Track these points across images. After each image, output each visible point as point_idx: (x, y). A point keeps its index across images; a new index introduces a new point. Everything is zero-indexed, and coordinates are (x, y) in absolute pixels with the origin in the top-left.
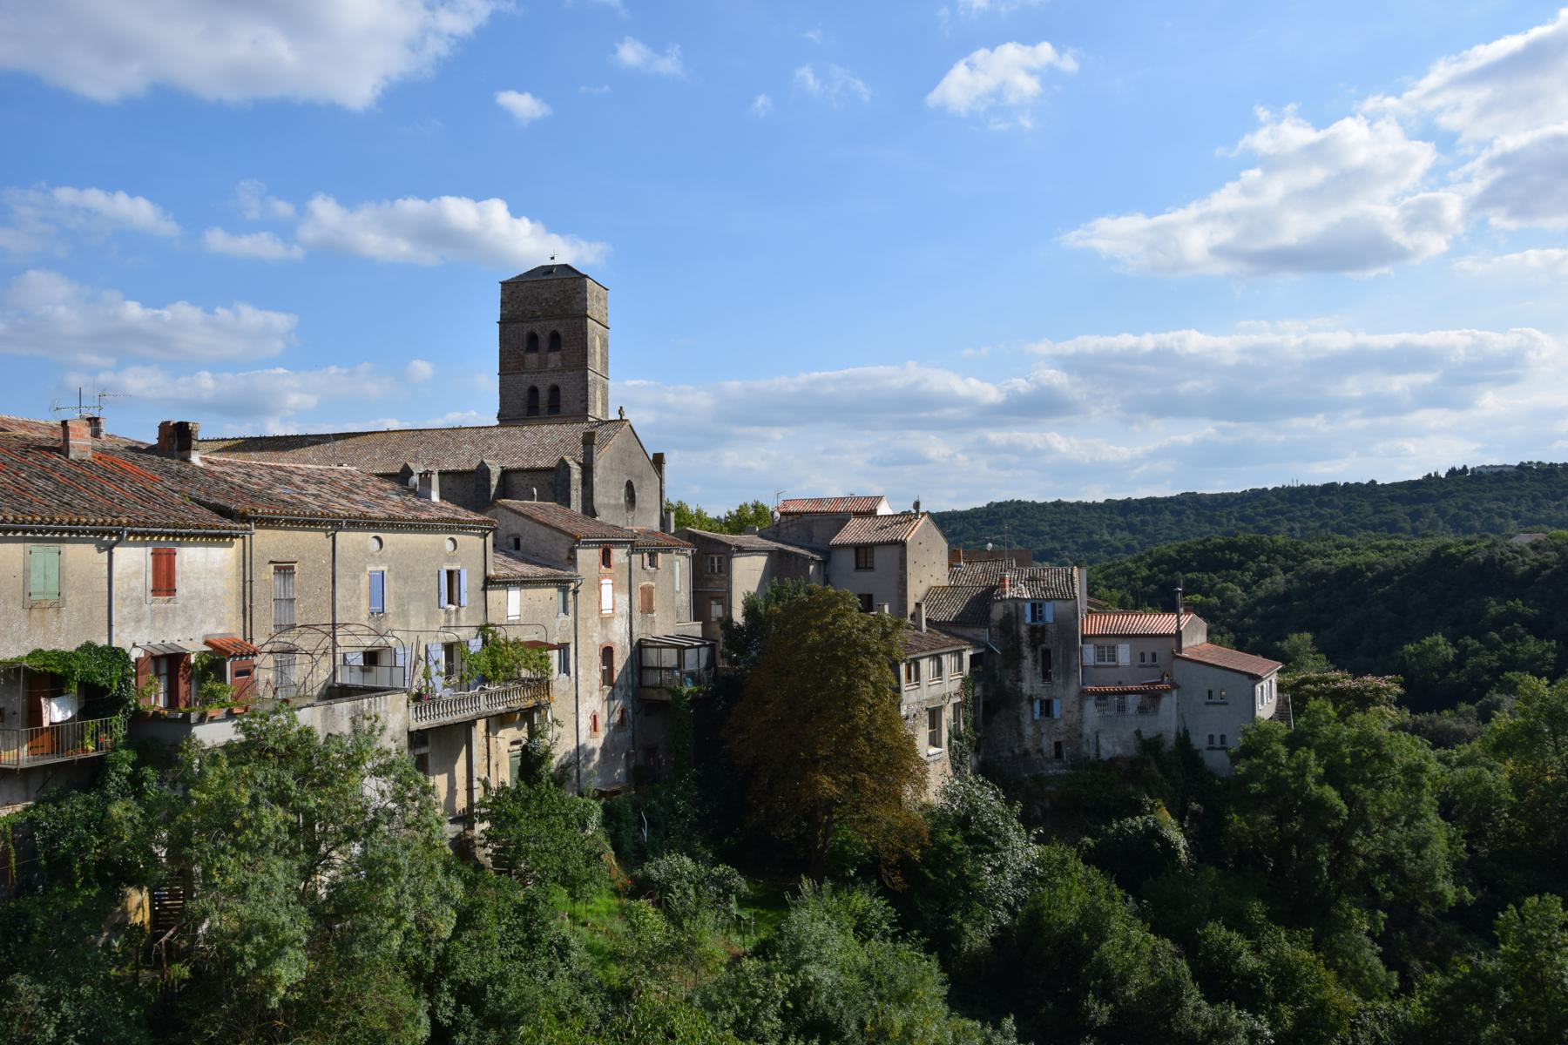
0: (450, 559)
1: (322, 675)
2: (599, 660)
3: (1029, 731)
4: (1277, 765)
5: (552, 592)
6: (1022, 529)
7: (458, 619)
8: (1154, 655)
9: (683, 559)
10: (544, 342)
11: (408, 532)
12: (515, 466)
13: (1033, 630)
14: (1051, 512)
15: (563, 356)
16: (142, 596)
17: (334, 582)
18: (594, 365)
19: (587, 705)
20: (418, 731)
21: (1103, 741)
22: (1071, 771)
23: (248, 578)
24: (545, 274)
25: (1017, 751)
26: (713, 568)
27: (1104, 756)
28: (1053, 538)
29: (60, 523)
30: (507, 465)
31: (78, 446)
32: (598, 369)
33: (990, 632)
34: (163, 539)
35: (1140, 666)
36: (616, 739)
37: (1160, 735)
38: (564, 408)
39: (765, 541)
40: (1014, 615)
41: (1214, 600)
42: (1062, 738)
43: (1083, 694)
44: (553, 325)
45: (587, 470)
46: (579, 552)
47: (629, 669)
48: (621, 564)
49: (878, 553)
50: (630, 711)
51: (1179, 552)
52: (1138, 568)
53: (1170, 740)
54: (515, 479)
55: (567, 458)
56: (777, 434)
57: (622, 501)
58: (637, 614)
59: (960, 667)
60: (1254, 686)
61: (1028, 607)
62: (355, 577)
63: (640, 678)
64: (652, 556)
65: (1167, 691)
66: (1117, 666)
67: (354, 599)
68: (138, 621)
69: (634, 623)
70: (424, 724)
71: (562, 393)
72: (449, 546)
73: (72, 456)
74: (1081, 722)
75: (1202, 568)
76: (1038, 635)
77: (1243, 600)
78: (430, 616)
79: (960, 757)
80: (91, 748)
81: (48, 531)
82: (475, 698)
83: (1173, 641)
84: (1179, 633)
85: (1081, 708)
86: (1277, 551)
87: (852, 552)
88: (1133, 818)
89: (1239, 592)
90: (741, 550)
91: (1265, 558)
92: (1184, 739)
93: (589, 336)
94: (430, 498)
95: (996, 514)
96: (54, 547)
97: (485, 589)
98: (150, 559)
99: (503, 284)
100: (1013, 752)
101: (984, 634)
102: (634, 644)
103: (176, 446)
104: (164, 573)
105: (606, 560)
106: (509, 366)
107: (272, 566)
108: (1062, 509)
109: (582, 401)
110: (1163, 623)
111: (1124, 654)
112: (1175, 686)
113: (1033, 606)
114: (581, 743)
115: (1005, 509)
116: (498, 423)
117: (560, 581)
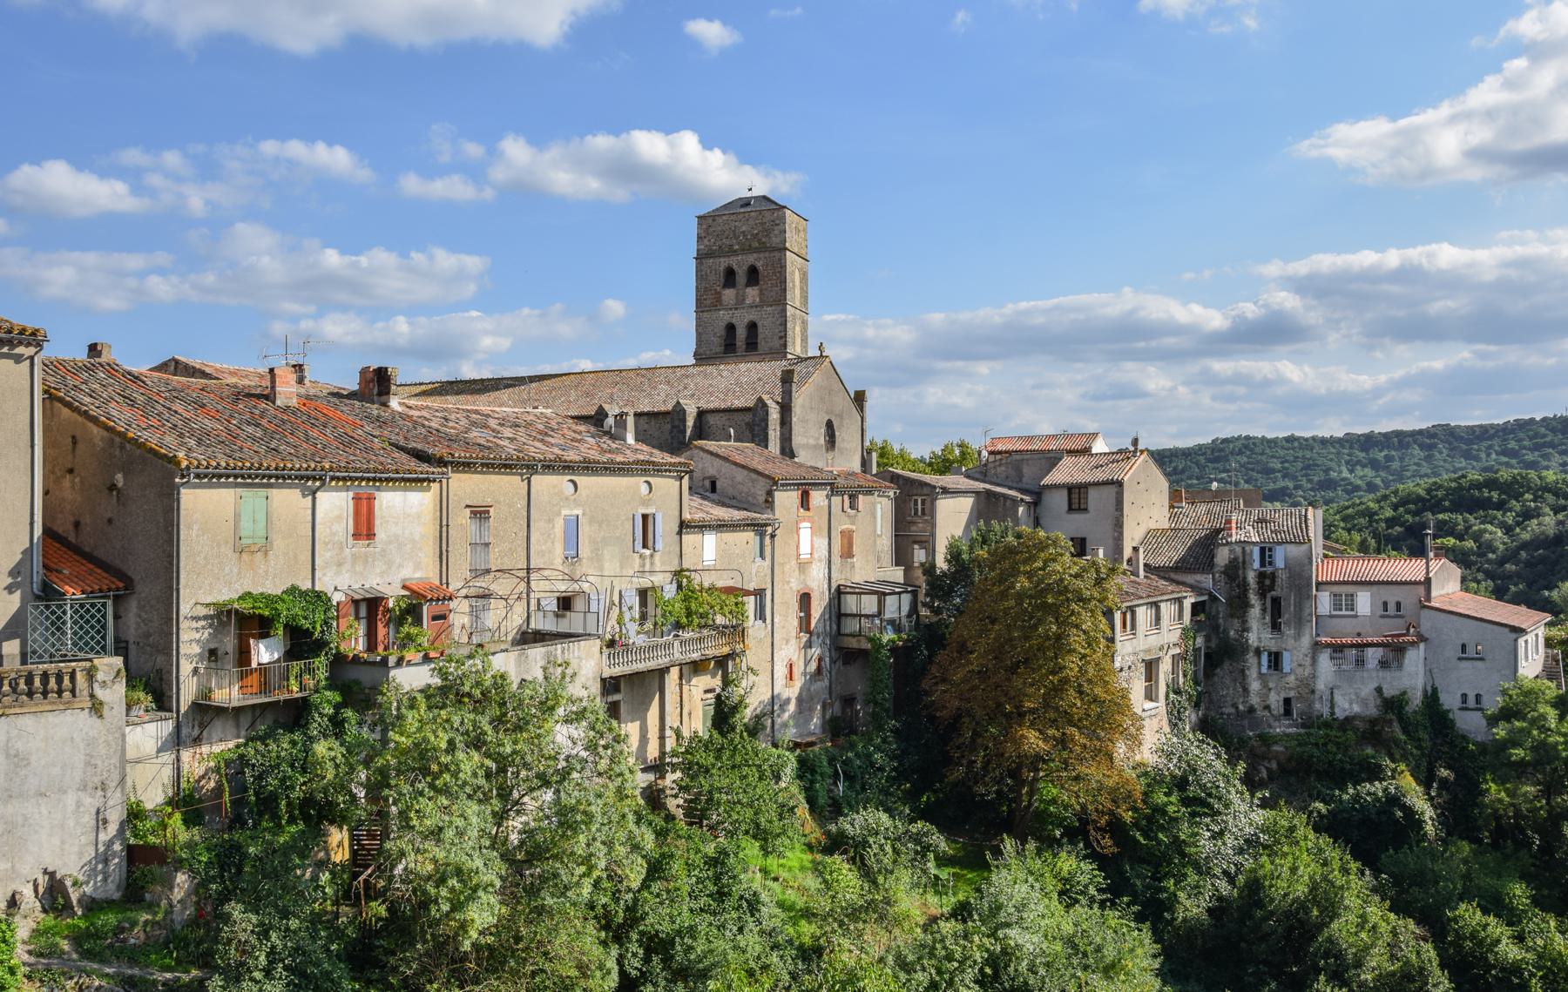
0: (645, 503)
2: (796, 606)
3: (1255, 686)
4: (1545, 729)
5: (749, 536)
7: (652, 564)
8: (1398, 605)
9: (885, 501)
10: (741, 278)
11: (602, 475)
12: (711, 406)
13: (1261, 576)
14: (1283, 448)
15: (761, 291)
16: (344, 540)
17: (528, 526)
18: (793, 299)
19: (783, 653)
20: (611, 678)
21: (1338, 698)
22: (1303, 731)
23: (444, 523)
24: (742, 206)
25: (1241, 707)
26: (916, 510)
27: (1340, 714)
28: (1284, 477)
29: (268, 469)
30: (704, 405)
31: (285, 393)
32: (797, 304)
33: (1213, 579)
34: (364, 483)
37: (1404, 693)
38: (762, 345)
39: (972, 482)
40: (1241, 560)
41: (1469, 544)
42: (1292, 694)
43: (1316, 646)
44: (751, 259)
45: (786, 409)
47: (827, 617)
49: (1093, 494)
51: (1429, 491)
52: (1381, 508)
53: (1416, 700)
55: (765, 397)
56: (983, 368)
57: (822, 441)
58: (836, 559)
60: (1516, 640)
62: (550, 521)
64: (853, 497)
65: (1413, 644)
66: (1356, 616)
67: (549, 544)
68: (340, 565)
69: (833, 567)
70: (617, 671)
71: (760, 330)
72: (644, 489)
73: (278, 402)
74: (1314, 676)
75: (1457, 507)
76: (1267, 582)
77: (1504, 543)
78: (624, 562)
79: (1179, 712)
80: (295, 689)
81: (257, 477)
82: (668, 646)
83: (1421, 590)
84: (1428, 581)
85: (1314, 661)
86: (1546, 489)
87: (1065, 493)
88: (1371, 783)
89: (1500, 534)
90: (945, 491)
91: (1531, 497)
92: (1432, 698)
94: (624, 440)
95: (1222, 450)
96: (262, 492)
97: (680, 533)
98: (351, 503)
100: (1237, 708)
101: (1207, 580)
103: (376, 391)
104: (364, 518)
105: (805, 502)
106: (706, 302)
107: (468, 510)
108: (1296, 444)
109: (781, 338)
110: (1408, 569)
111: (1364, 602)
113: (1262, 550)
114: (776, 693)
115: (1231, 446)
117: (758, 525)
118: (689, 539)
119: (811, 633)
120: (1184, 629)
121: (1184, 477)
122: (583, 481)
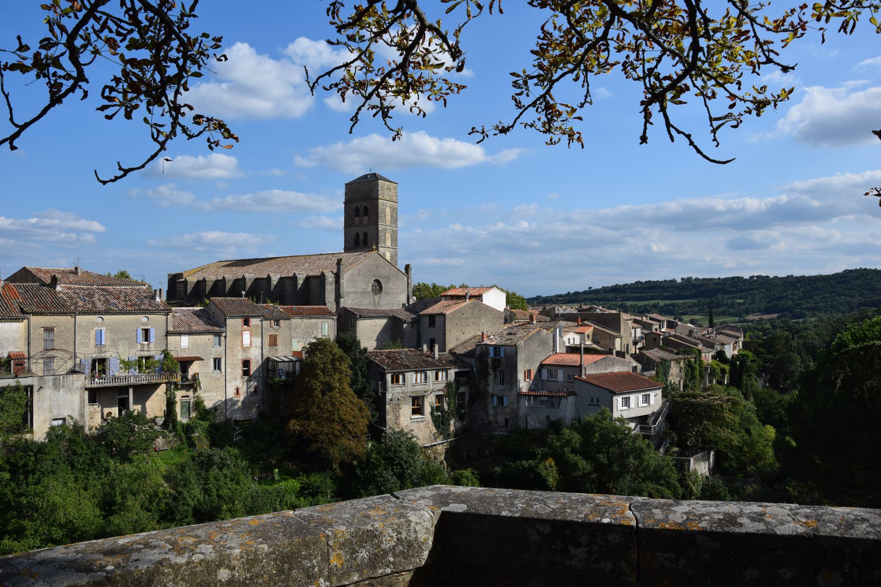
0: (143, 324)
1: (70, 365)
2: (241, 365)
3: (491, 412)
5: (211, 337)
6: (863, 286)
9: (330, 321)
10: (361, 212)
12: (313, 274)
13: (494, 360)
21: (529, 420)
25: (485, 421)
27: (530, 428)
30: (311, 274)
35: (568, 382)
37: (560, 420)
42: (508, 417)
44: (365, 203)
45: (337, 276)
50: (261, 388)
54: (313, 281)
57: (370, 289)
59: (447, 377)
61: (491, 350)
62: (88, 332)
63: (268, 374)
70: (95, 386)
71: (369, 236)
74: (518, 409)
76: (497, 363)
84: (581, 366)
95: (846, 277)
99: (346, 185)
101: (473, 361)
102: (264, 359)
105: (246, 323)
111: (561, 375)
112: (573, 393)
115: (852, 274)
116: (343, 251)
118: (171, 339)
119: (250, 377)
120: (447, 384)
122: (105, 317)
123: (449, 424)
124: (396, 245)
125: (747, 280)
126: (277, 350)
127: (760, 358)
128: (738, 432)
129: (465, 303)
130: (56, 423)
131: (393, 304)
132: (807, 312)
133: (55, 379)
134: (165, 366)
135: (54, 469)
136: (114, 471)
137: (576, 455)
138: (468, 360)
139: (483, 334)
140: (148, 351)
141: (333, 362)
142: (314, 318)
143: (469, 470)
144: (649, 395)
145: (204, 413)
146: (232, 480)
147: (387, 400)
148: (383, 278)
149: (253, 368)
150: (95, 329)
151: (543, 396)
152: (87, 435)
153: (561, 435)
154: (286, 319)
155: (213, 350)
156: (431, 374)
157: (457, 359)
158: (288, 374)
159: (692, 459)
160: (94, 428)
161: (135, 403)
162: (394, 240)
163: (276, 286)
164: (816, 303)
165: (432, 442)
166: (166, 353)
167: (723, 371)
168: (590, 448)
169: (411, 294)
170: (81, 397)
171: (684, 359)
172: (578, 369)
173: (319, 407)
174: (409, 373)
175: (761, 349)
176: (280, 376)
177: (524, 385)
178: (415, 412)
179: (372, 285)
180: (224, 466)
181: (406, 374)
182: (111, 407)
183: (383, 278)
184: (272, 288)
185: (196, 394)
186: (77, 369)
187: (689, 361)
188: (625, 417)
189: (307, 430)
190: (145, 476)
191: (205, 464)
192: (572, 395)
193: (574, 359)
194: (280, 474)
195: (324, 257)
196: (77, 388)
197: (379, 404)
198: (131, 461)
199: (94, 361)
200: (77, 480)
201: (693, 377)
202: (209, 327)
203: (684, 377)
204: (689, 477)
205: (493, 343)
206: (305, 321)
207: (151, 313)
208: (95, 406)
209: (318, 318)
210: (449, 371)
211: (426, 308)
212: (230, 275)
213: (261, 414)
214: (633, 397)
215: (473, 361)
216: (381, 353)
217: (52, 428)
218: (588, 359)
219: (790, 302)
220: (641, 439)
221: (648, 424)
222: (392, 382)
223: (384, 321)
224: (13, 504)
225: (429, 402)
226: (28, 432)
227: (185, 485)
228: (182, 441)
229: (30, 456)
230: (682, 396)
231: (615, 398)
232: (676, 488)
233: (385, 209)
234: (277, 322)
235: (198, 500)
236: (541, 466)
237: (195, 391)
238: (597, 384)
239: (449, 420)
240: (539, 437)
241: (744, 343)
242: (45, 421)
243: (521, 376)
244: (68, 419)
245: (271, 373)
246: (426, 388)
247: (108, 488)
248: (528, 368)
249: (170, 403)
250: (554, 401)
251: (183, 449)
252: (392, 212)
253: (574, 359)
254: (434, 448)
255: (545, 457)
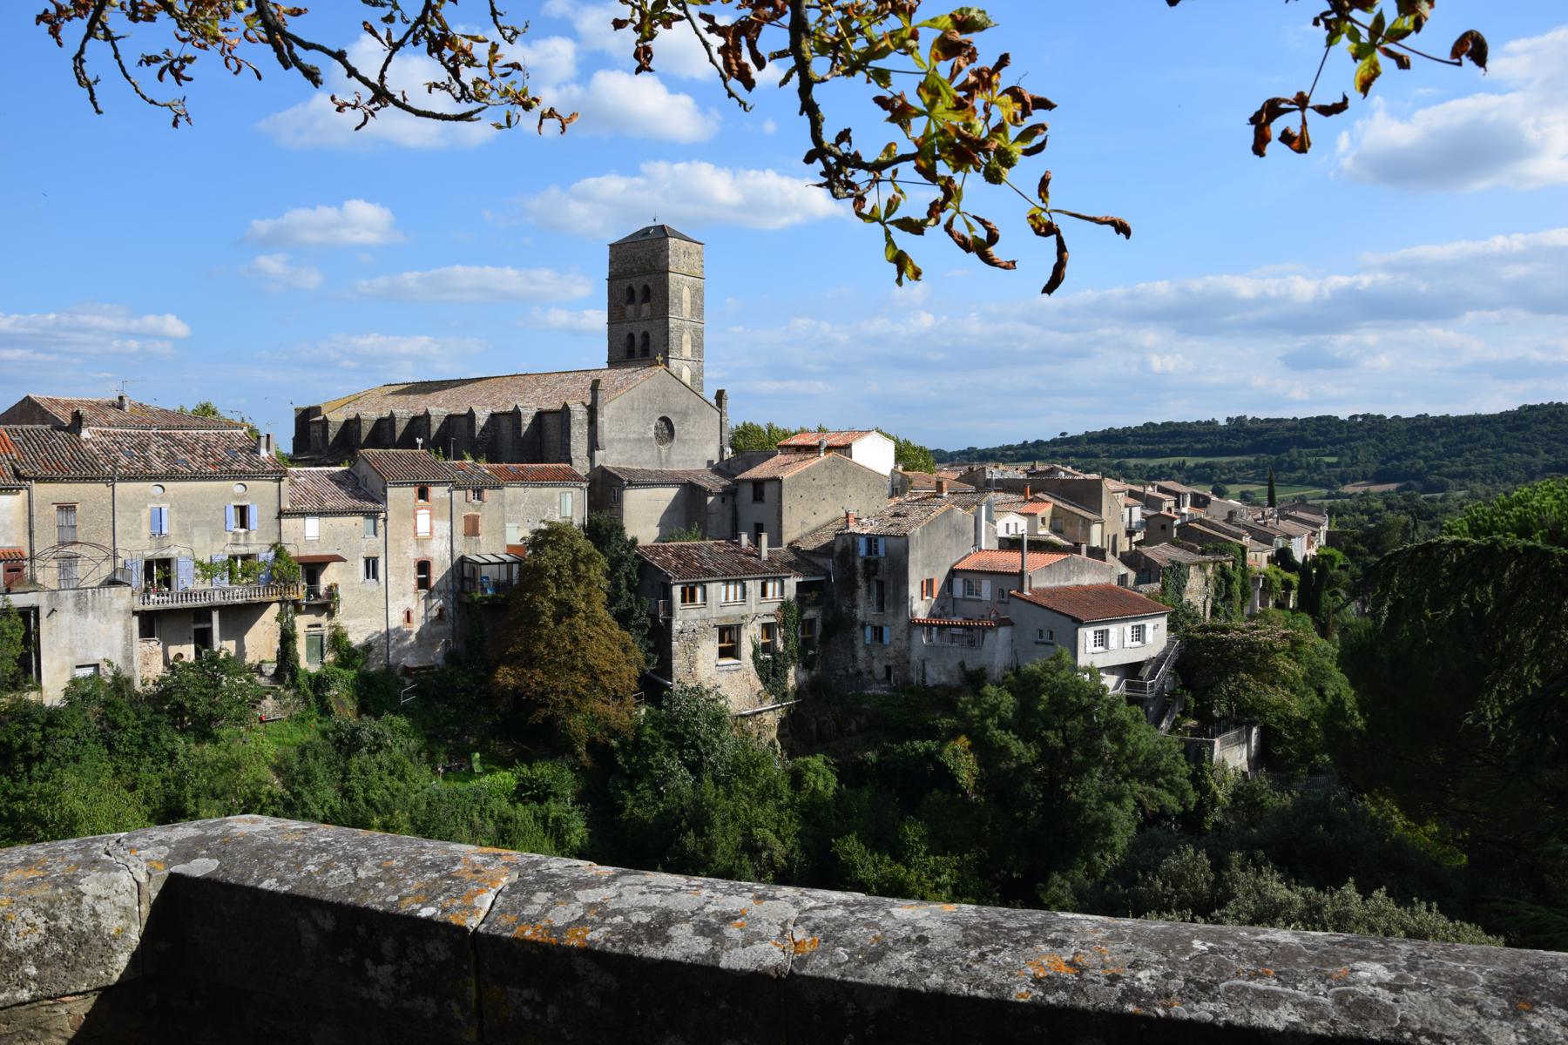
0: (237, 497)
1: (106, 570)
2: (414, 570)
3: (861, 654)
5: (360, 519)
6: (1553, 436)
9: (576, 491)
10: (638, 296)
13: (867, 562)
19: (400, 603)
21: (928, 669)
25: (851, 670)
27: (929, 682)
30: (546, 407)
35: (999, 602)
36: (433, 630)
37: (982, 669)
42: (891, 663)
44: (645, 280)
45: (592, 411)
46: (389, 490)
47: (449, 578)
48: (442, 499)
55: (569, 403)
57: (652, 434)
59: (782, 592)
61: (862, 544)
70: (151, 607)
74: (909, 649)
76: (872, 568)
84: (1022, 573)
93: (671, 287)
95: (1524, 418)
97: (279, 518)
99: (611, 246)
101: (829, 564)
102: (455, 559)
105: (423, 494)
111: (986, 589)
112: (1007, 623)
115: (1535, 413)
116: (606, 366)
118: (287, 523)
119: (431, 590)
120: (783, 603)
121: (1479, 445)
122: (167, 485)
123: (786, 676)
124: (701, 356)
125: (1344, 421)
126: (478, 543)
127: (1357, 561)
128: (1303, 694)
129: (817, 460)
130: (80, 673)
131: (693, 461)
132: (1450, 481)
133: (79, 596)
134: (275, 573)
135: (78, 753)
136: (185, 756)
137: (1007, 733)
138: (821, 562)
139: (847, 515)
140: (246, 545)
141: (574, 566)
142: (547, 485)
143: (820, 757)
144: (1144, 626)
145: (348, 655)
146: (391, 773)
147: (675, 633)
148: (675, 413)
149: (436, 575)
150: (150, 506)
151: (953, 626)
152: (138, 694)
153: (981, 696)
154: (494, 488)
155: (364, 543)
156: (753, 587)
157: (801, 559)
158: (498, 586)
159: (1217, 742)
160: (151, 682)
161: (223, 637)
162: (698, 345)
163: (483, 429)
164: (1468, 465)
165: (755, 707)
166: (279, 550)
167: (1287, 585)
168: (1032, 720)
169: (726, 442)
170: (125, 627)
171: (1214, 563)
172: (1017, 579)
173: (549, 645)
174: (714, 585)
175: (1359, 547)
176: (484, 590)
177: (920, 607)
178: (724, 653)
179: (656, 427)
180: (380, 747)
181: (708, 585)
182: (181, 643)
183: (675, 413)
184: (477, 433)
185: (334, 622)
186: (118, 577)
187: (1223, 567)
188: (1098, 665)
189: (529, 686)
190: (237, 766)
191: (347, 744)
192: (1004, 625)
193: (1010, 560)
194: (482, 763)
195: (571, 376)
196: (119, 612)
197: (659, 638)
198: (215, 740)
199: (149, 565)
200: (120, 773)
201: (1229, 596)
202: (357, 503)
203: (1212, 594)
204: (1211, 772)
205: (865, 532)
206: (531, 490)
207: (251, 477)
208: (152, 643)
209: (554, 485)
210: (786, 582)
211: (750, 467)
212: (405, 409)
213: (451, 657)
214: (1114, 630)
215: (829, 564)
216: (665, 548)
217: (75, 682)
218: (1035, 561)
219: (1422, 462)
220: (1123, 705)
221: (1141, 678)
222: (684, 600)
223: (672, 492)
224: (5, 814)
225: (750, 636)
226: (33, 689)
227: (307, 782)
228: (309, 704)
229: (34, 730)
230: (1204, 629)
231: (1081, 631)
232: (1184, 792)
233: (680, 290)
234: (479, 492)
235: (331, 808)
236: (947, 751)
237: (331, 614)
238: (1050, 605)
239: (786, 668)
240: (944, 699)
241: (1329, 535)
242: (62, 670)
243: (914, 590)
244: (103, 665)
245: (467, 584)
246: (744, 610)
247: (173, 786)
248: (927, 576)
249: (287, 638)
250: (972, 635)
251: (310, 718)
252: (693, 296)
253: (1010, 560)
254: (759, 717)
255: (954, 734)
